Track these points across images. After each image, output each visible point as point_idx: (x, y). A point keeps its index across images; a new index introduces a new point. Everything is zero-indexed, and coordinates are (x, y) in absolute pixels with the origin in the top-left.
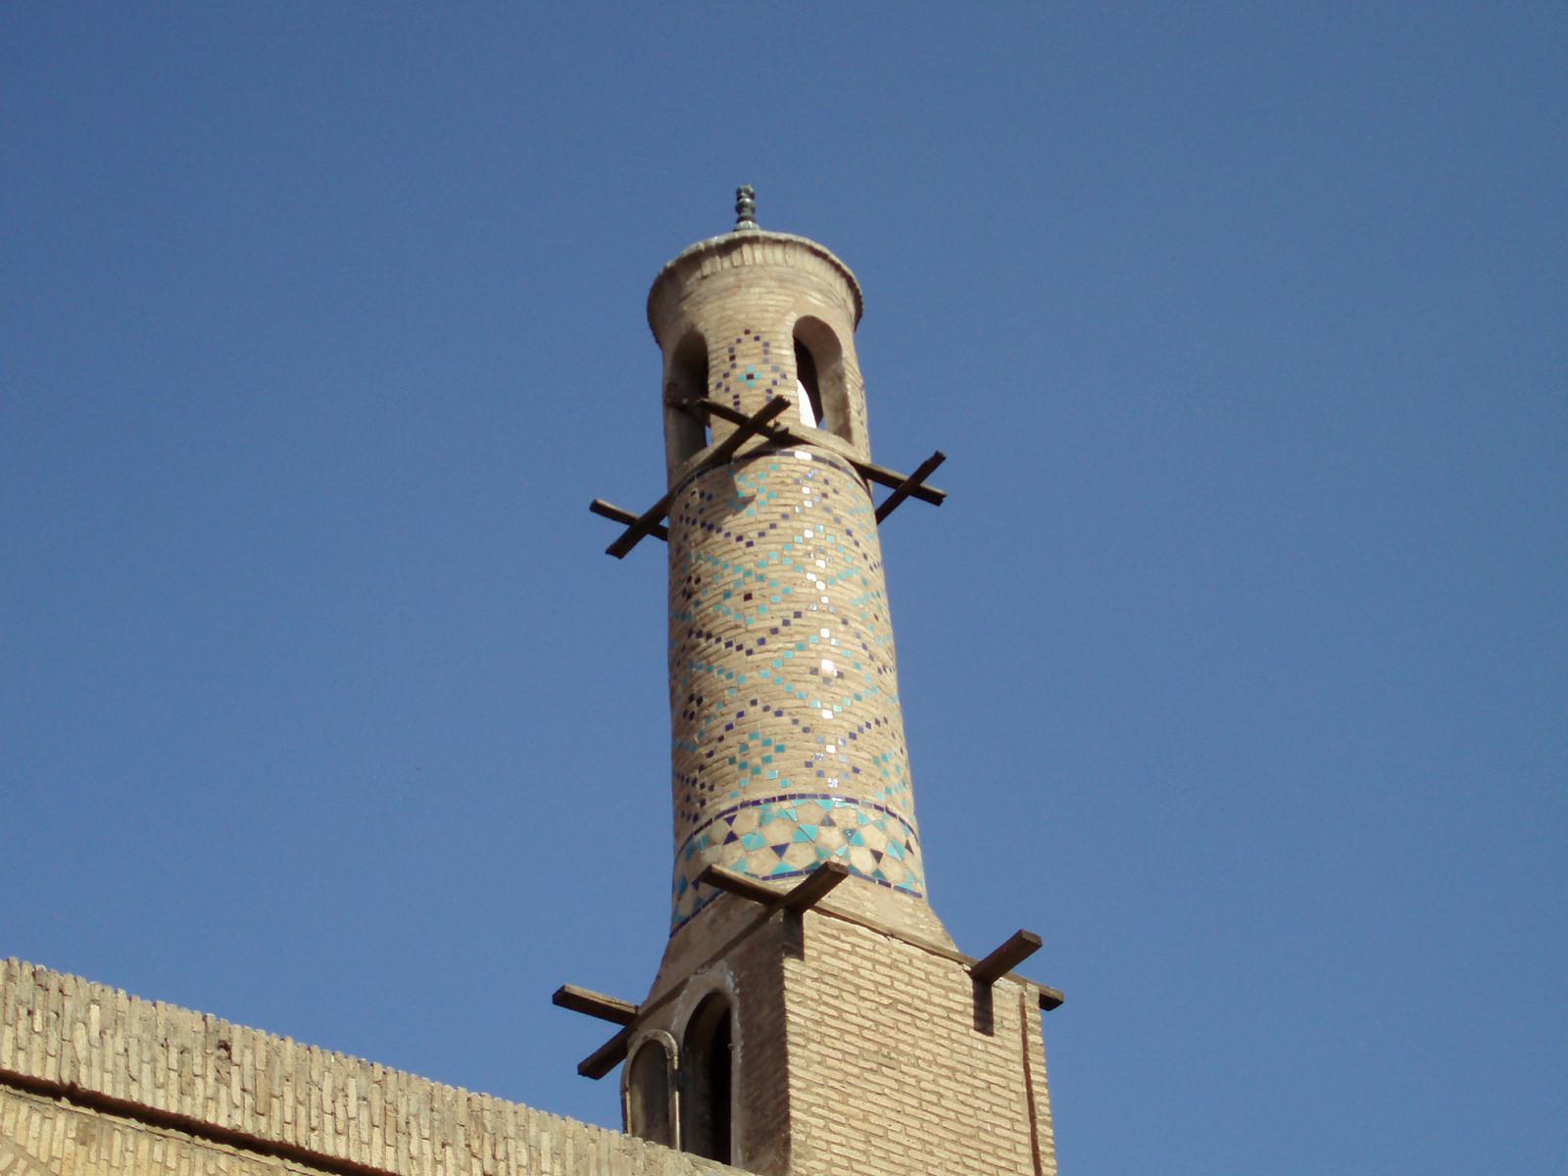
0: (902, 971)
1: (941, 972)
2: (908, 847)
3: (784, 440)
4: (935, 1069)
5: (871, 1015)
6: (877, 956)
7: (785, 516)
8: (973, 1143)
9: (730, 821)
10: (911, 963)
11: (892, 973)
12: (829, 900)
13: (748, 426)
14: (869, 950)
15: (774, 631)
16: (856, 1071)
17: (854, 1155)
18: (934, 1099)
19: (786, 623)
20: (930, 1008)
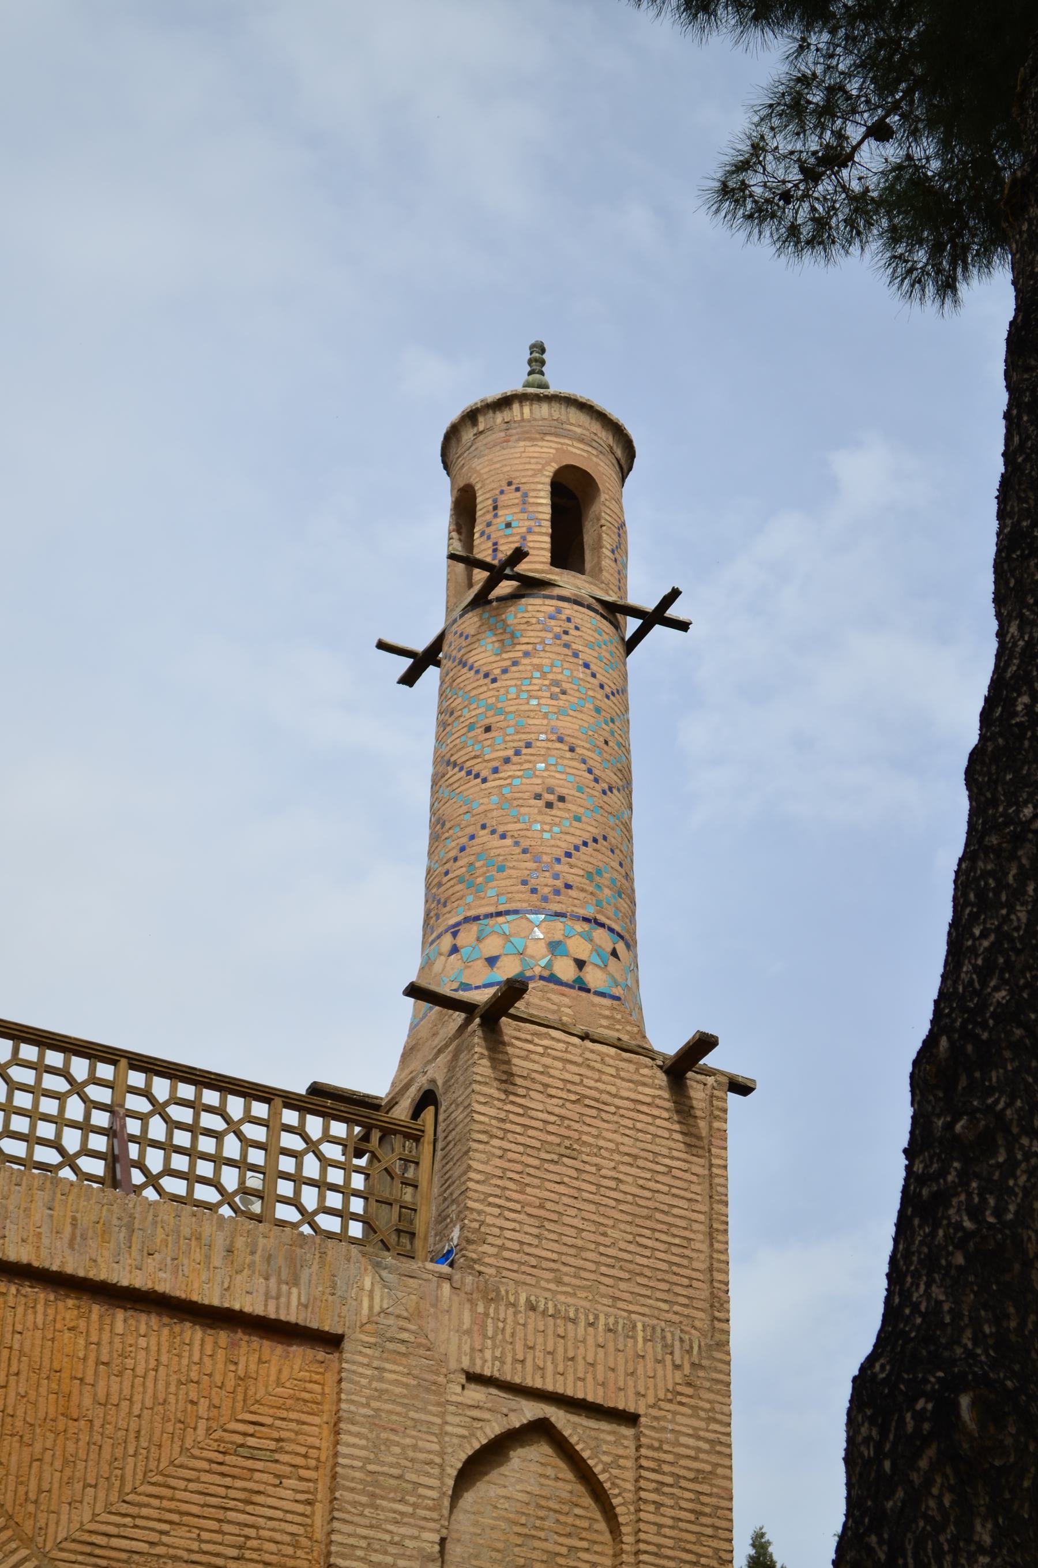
0: (593, 1068)
1: (632, 1068)
2: (614, 953)
3: (531, 585)
4: (616, 1157)
5: (557, 1110)
6: (569, 1057)
7: (527, 654)
8: (648, 1223)
9: (455, 934)
10: (603, 1061)
11: (583, 1071)
12: (520, 1007)
13: (497, 574)
14: (561, 1051)
15: (507, 760)
16: (536, 1162)
17: (528, 1239)
18: (612, 1184)
19: (517, 753)
20: (618, 1102)
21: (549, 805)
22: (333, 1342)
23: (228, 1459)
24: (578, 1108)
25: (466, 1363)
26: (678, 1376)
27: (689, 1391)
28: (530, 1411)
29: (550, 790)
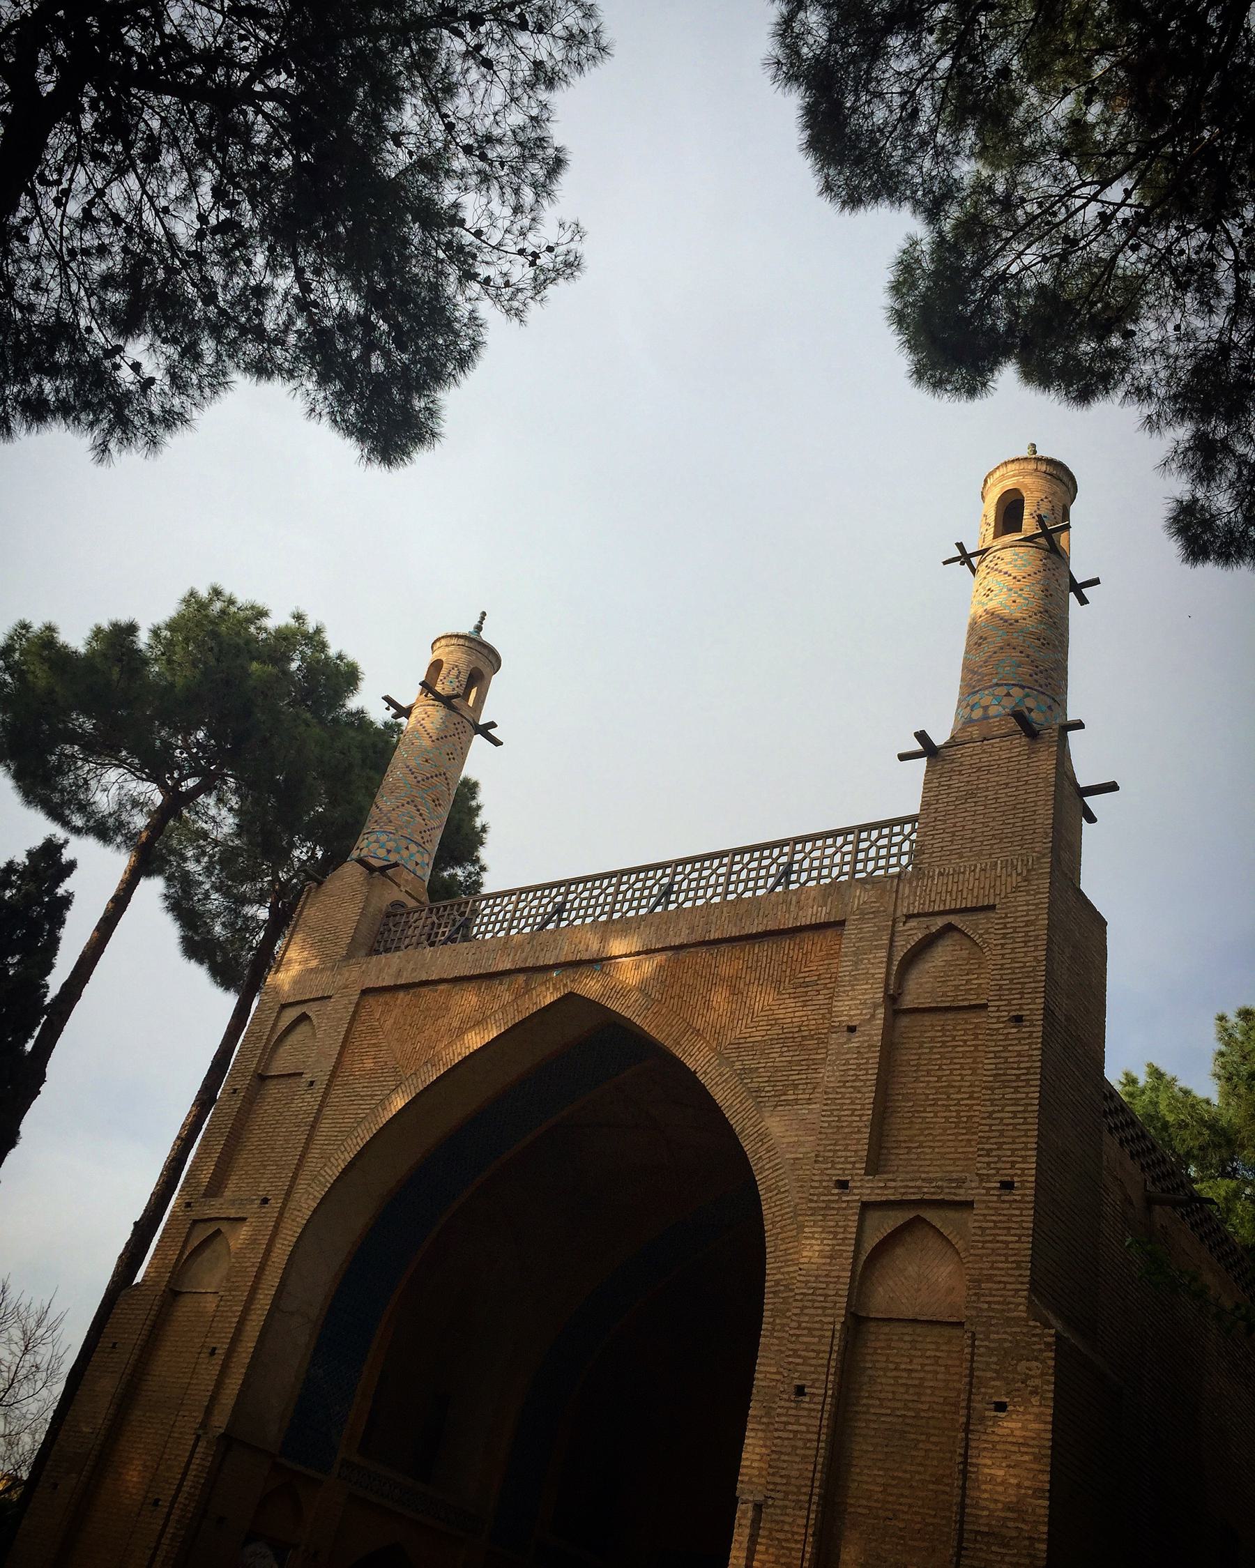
21: (980, 645)
22: (841, 923)
23: (798, 990)
24: (977, 774)
25: (905, 911)
26: (1019, 879)
27: (1026, 883)
28: (940, 922)
29: (981, 638)
